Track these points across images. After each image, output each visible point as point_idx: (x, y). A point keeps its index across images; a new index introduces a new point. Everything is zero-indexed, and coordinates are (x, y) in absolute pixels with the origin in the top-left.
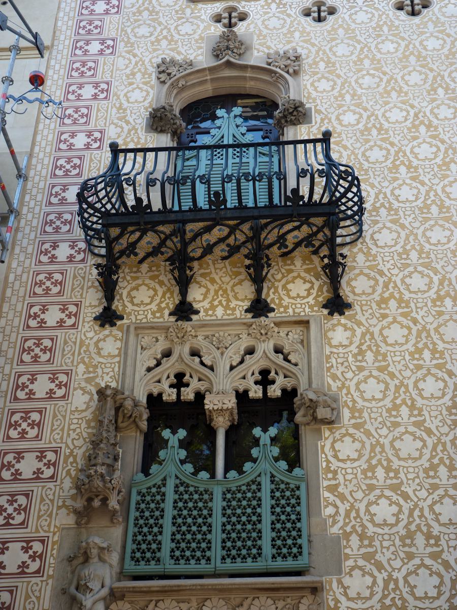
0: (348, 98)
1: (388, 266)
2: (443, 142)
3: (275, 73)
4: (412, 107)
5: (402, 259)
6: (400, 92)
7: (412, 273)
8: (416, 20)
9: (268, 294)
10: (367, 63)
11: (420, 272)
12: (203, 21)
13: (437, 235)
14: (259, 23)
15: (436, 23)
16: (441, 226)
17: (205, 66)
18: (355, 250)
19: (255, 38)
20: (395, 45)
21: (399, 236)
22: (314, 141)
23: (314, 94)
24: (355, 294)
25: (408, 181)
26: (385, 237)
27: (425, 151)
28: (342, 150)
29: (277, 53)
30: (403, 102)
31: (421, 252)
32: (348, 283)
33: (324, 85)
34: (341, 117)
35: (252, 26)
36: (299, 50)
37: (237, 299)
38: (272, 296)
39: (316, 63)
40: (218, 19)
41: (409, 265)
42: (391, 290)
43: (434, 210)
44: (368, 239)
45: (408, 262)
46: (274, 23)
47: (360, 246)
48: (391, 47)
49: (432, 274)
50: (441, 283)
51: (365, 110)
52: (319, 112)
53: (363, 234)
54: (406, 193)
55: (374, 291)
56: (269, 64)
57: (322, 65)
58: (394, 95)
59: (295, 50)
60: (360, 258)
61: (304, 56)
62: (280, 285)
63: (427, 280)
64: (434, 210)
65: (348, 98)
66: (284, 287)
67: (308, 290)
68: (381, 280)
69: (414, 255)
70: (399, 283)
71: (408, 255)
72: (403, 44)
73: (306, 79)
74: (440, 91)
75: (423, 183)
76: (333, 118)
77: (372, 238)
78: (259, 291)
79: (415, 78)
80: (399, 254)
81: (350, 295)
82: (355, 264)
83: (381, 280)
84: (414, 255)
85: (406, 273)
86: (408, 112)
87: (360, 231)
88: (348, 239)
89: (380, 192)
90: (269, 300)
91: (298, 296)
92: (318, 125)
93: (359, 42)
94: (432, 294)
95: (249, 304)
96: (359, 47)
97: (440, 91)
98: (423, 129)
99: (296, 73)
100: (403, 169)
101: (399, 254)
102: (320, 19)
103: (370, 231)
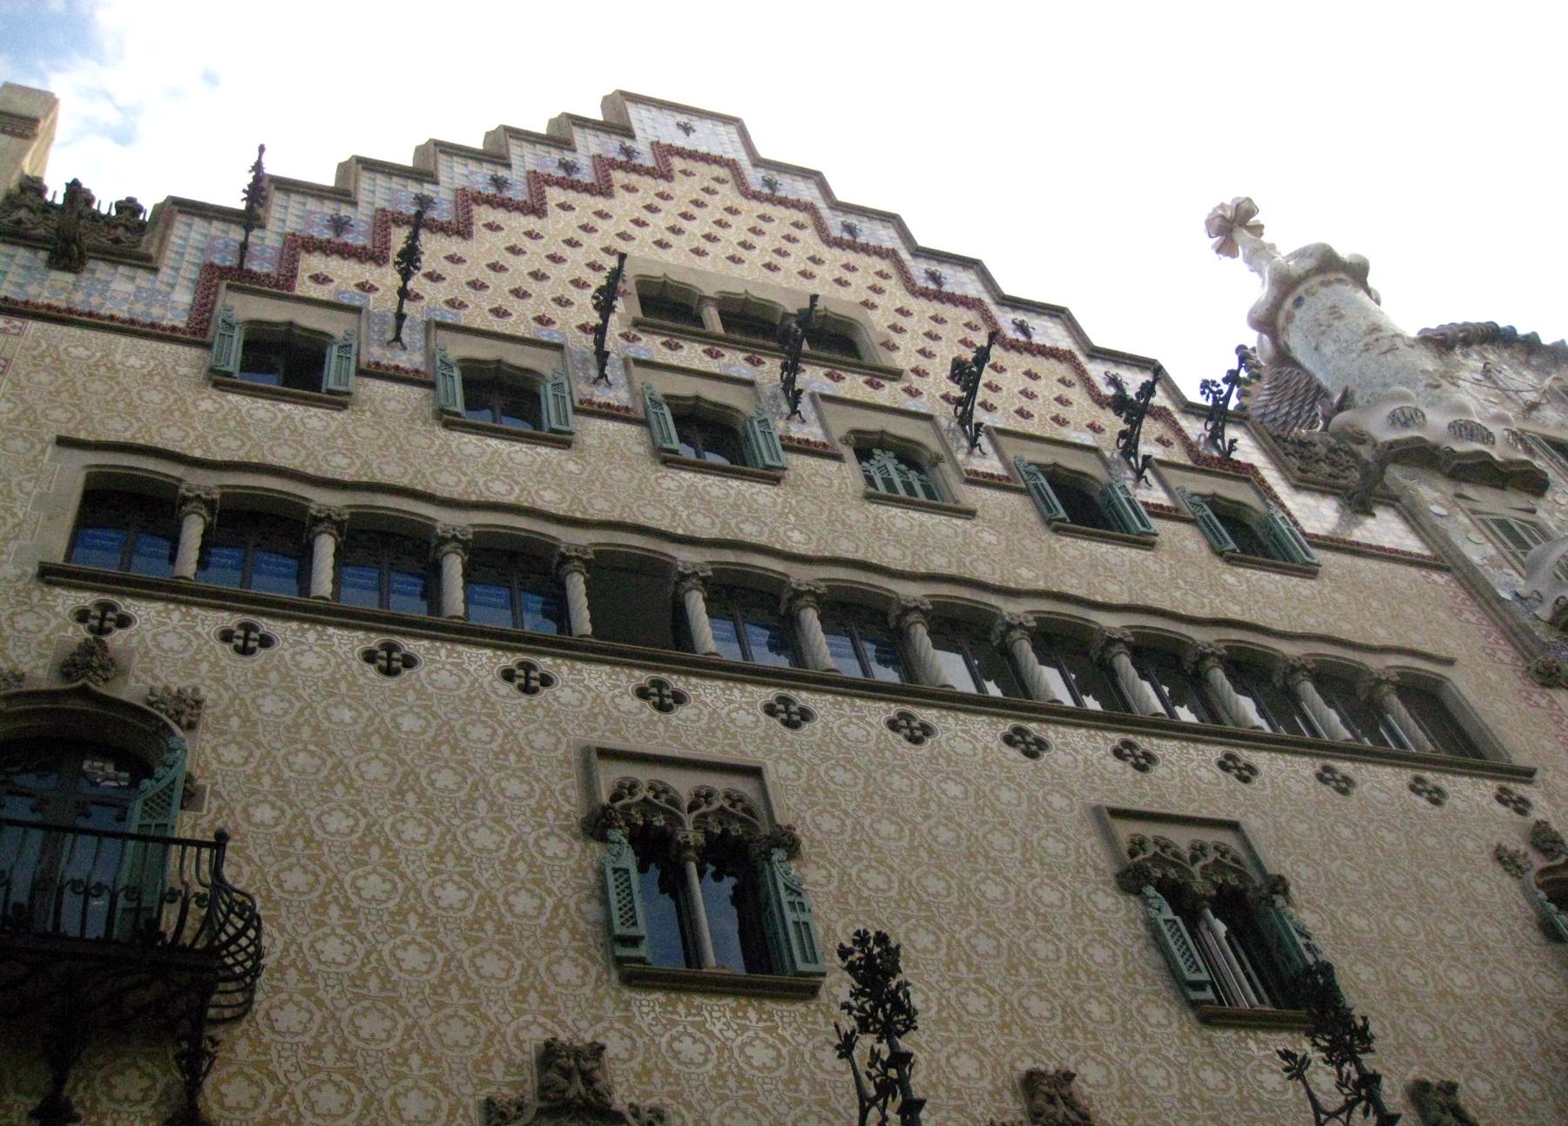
0: (267, 780)
1: (286, 1066)
2: (402, 876)
3: (158, 719)
4: (365, 813)
5: (309, 1057)
6: (349, 787)
7: (322, 1082)
8: (391, 683)
9: (74, 1090)
11: (335, 1084)
12: (57, 615)
13: (371, 1025)
15: (421, 693)
17: (44, 686)
18: (237, 1032)
19: (137, 658)
20: (354, 714)
21: (311, 1019)
22: (200, 844)
23: (214, 765)
24: (222, 1105)
25: (340, 931)
26: (289, 1018)
27: (373, 885)
28: (243, 863)
29: (167, 689)
30: (353, 804)
31: (342, 1050)
32: (216, 1088)
33: (232, 754)
34: (251, 810)
35: (135, 640)
36: (203, 691)
37: (17, 1090)
38: (80, 1093)
40: (82, 616)
41: (319, 1069)
42: (284, 1107)
43: (374, 983)
44: (259, 1017)
45: (320, 1063)
46: (170, 641)
47: (244, 1025)
48: (347, 715)
49: (354, 1089)
51: (292, 804)
52: (216, 795)
53: (255, 1007)
54: (333, 949)
55: (256, 1105)
56: (151, 704)
58: (340, 788)
59: (196, 690)
60: (243, 1048)
61: (208, 702)
62: (100, 1074)
63: (344, 1098)
64: (374, 983)
66: (106, 1081)
67: (146, 1091)
68: (271, 1090)
69: (330, 1054)
70: (299, 1097)
71: (321, 1052)
72: (366, 714)
74: (411, 797)
75: (362, 938)
77: (267, 1014)
78: (59, 1082)
79: (375, 770)
80: (307, 1049)
81: (215, 1106)
82: (232, 1056)
83: (271, 1090)
84: (330, 1054)
85: (313, 1081)
86: (357, 820)
87: (250, 1002)
88: (228, 1013)
89: (293, 941)
90: (74, 1100)
91: (127, 1098)
92: (212, 816)
93: (299, 698)
95: (38, 1102)
96: (298, 705)
97: (411, 797)
98: (375, 851)
99: (191, 726)
100: (334, 911)
101: (307, 1049)
102: (245, 651)
103: (266, 1005)
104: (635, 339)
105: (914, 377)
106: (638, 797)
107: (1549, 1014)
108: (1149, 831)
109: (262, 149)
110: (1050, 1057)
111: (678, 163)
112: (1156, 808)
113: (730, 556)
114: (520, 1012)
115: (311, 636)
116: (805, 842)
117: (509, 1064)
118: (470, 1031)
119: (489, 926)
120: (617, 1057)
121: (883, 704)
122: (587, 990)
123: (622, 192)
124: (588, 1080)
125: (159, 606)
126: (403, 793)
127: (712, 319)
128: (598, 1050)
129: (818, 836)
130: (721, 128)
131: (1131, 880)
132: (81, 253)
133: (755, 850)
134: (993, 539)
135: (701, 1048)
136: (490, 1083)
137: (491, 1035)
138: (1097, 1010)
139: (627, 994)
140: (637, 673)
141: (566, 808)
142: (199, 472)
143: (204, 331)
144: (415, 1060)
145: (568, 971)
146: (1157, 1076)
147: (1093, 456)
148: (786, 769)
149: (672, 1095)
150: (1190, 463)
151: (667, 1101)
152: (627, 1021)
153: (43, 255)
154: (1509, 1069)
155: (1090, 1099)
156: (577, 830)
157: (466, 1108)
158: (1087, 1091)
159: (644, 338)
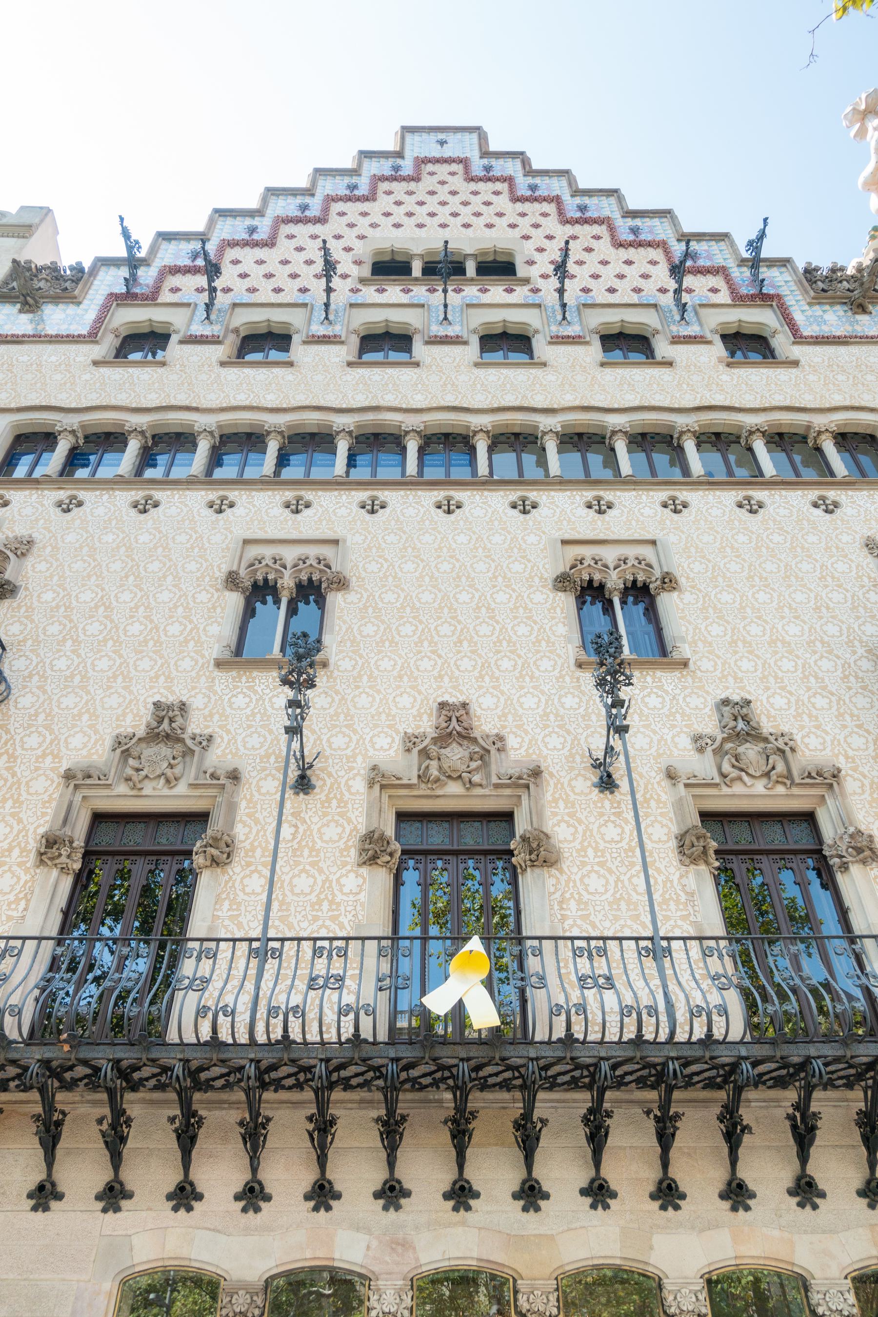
2: (112, 621)
4: (103, 590)
10: (85, 549)
14: (16, 510)
16: (76, 693)
23: (31, 573)
26: (26, 701)
39: (44, 547)
43: (77, 679)
44: (12, 703)
46: (28, 511)
50: (51, 743)
52: (27, 589)
57: (49, 549)
64: (77, 679)
65: (56, 578)
73: (30, 561)
76: (36, 594)
84: (42, 717)
94: (39, 752)
97: (131, 578)
104: (358, 290)
105: (540, 280)
106: (264, 563)
107: (861, 651)
108: (587, 552)
109: (122, 219)
110: (462, 692)
111: (430, 167)
112: (602, 537)
113: (370, 416)
114: (151, 688)
115: (105, 497)
116: (354, 579)
117: (135, 716)
118: (121, 700)
119: (151, 643)
120: (197, 709)
121: (435, 493)
122: (193, 674)
123: (385, 196)
124: (171, 721)
125: (27, 492)
126: (127, 577)
127: (417, 269)
128: (183, 707)
129: (363, 574)
130: (467, 136)
131: (562, 582)
132: (36, 302)
133: (324, 586)
134: (553, 378)
135: (247, 700)
136: (122, 726)
137: (130, 702)
138: (506, 664)
139: (217, 673)
140: (287, 493)
141: (218, 574)
142: (71, 415)
143: (96, 334)
144: (85, 717)
145: (186, 664)
146: (530, 702)
147: (653, 310)
148: (358, 538)
149: (220, 727)
150: (729, 302)
151: (217, 730)
152: (210, 688)
153: (18, 306)
154: (809, 689)
155: (479, 717)
156: (219, 586)
157: (104, 741)
158: (479, 712)
159: (364, 289)
